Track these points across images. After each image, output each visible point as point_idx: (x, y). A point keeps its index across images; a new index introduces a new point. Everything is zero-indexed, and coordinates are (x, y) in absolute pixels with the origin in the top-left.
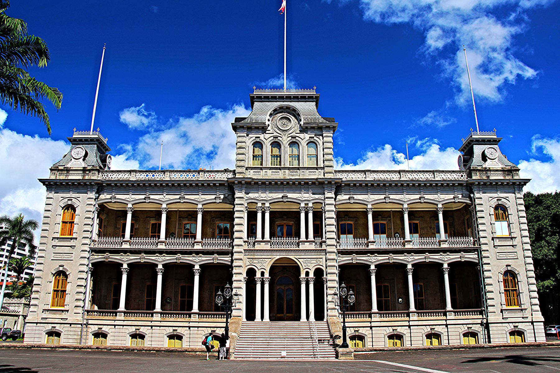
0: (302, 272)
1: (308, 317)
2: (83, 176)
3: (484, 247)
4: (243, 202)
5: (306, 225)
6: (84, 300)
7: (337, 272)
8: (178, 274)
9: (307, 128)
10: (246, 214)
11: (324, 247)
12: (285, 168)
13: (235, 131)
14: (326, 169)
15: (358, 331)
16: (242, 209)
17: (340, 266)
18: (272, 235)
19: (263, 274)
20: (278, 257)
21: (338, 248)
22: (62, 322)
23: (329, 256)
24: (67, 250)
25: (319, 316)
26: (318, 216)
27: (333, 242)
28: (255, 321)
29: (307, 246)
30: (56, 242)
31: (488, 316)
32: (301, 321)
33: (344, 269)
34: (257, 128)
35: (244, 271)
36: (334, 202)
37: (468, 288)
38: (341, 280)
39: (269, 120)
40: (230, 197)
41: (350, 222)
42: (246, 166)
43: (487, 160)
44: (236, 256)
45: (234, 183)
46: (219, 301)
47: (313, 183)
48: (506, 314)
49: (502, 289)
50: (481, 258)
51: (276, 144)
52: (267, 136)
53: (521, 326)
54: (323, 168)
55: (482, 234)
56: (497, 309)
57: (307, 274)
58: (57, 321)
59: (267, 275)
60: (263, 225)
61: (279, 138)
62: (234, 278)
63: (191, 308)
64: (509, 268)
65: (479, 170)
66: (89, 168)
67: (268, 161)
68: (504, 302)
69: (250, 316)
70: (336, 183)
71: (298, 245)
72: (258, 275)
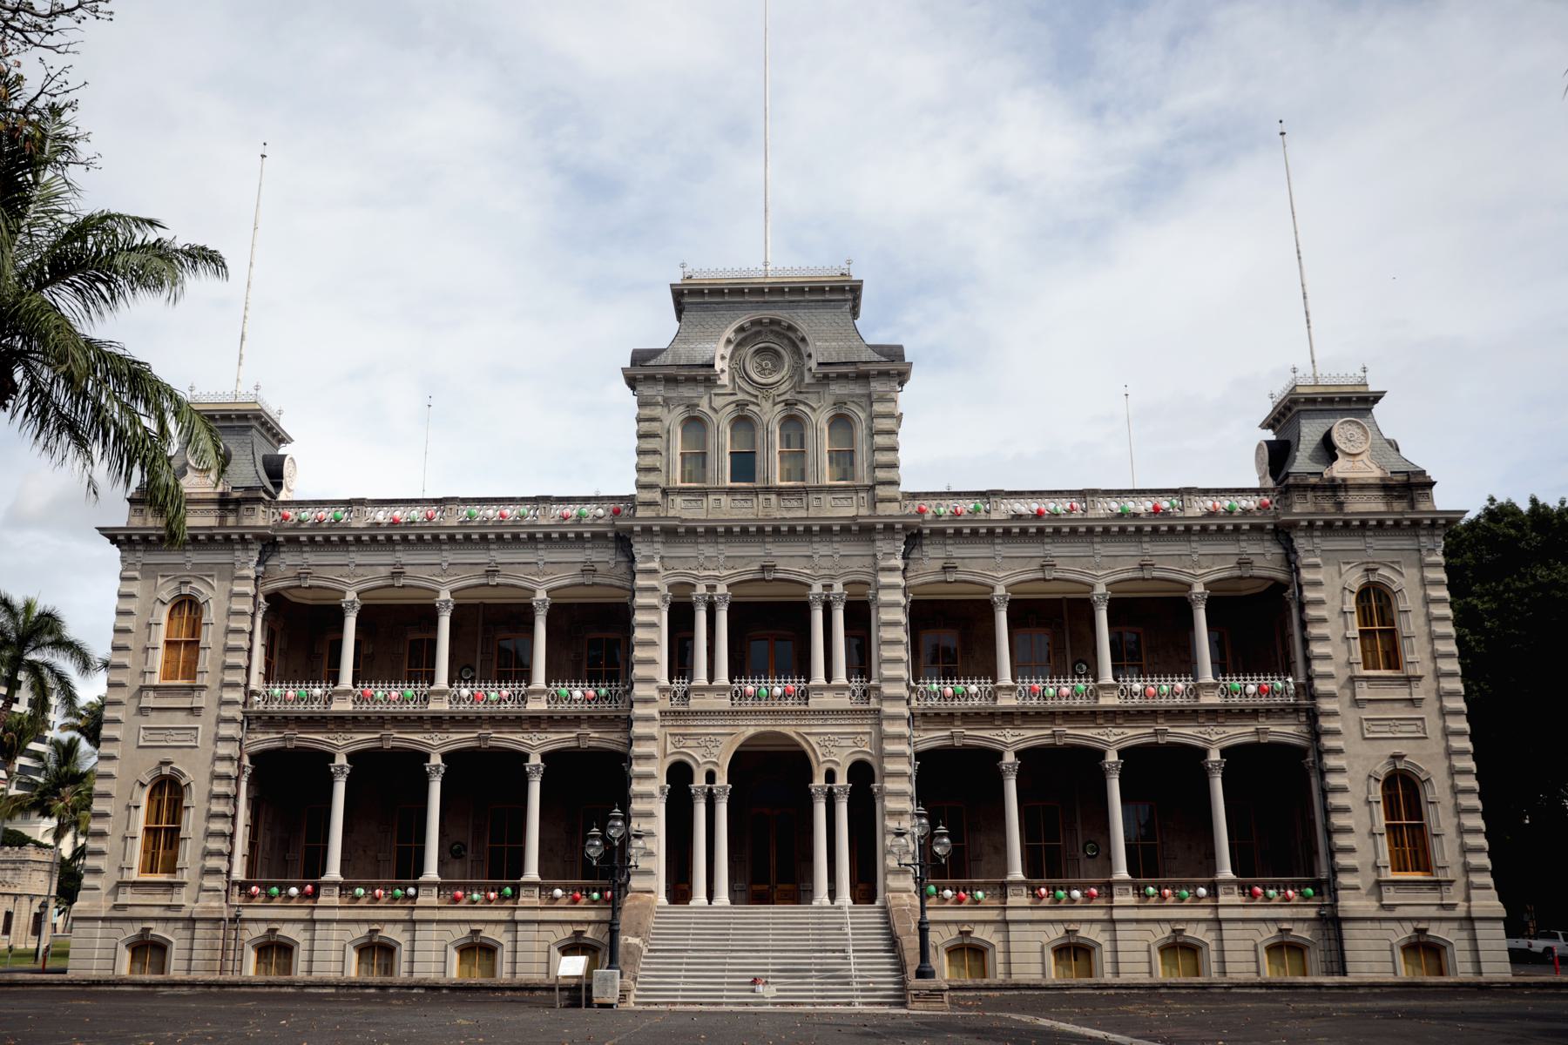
0: (816, 771)
1: (832, 894)
2: (222, 518)
3: (1325, 705)
4: (654, 583)
5: (827, 641)
6: (230, 855)
7: (909, 770)
8: (485, 782)
9: (826, 376)
11: (874, 703)
12: (768, 490)
13: (633, 388)
14: (882, 491)
15: (968, 933)
16: (654, 601)
17: (918, 755)
18: (736, 671)
19: (711, 777)
20: (751, 731)
22: (170, 914)
23: (889, 728)
24: (180, 720)
25: (865, 887)
26: (859, 616)
27: (901, 690)
28: (692, 903)
29: (828, 701)
30: (150, 700)
31: (1336, 900)
32: (815, 903)
33: (928, 761)
34: (692, 380)
35: (659, 769)
36: (902, 582)
37: (1279, 818)
38: (924, 793)
39: (723, 358)
40: (623, 568)
41: (950, 632)
43: (1335, 458)
44: (638, 729)
45: (630, 530)
46: (594, 850)
47: (845, 530)
48: (1391, 896)
49: (1381, 822)
50: (1316, 734)
52: (718, 402)
53: (1435, 931)
54: (872, 488)
55: (1318, 667)
56: (1364, 880)
57: (830, 776)
58: (156, 912)
59: (722, 780)
60: (713, 643)
61: (751, 407)
62: (636, 787)
63: (519, 869)
64: (1401, 765)
65: (1314, 487)
66: (236, 495)
67: (722, 471)
68: (1385, 857)
69: (679, 890)
70: (906, 527)
71: (805, 695)
72: (700, 781)
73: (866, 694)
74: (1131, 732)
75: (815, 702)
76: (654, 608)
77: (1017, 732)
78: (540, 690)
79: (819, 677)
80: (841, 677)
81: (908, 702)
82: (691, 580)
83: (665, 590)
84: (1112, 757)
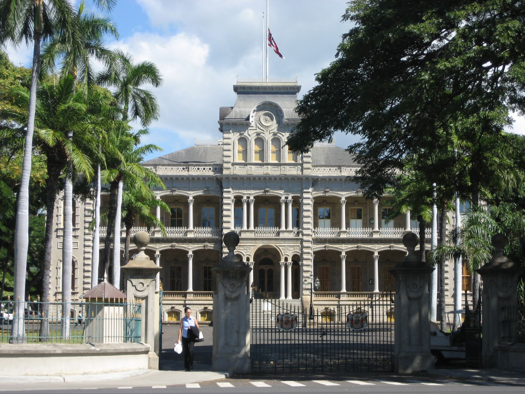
10: (233, 206)
12: (268, 164)
17: (314, 253)
18: (256, 225)
20: (261, 245)
21: (313, 236)
40: (218, 189)
42: (232, 162)
45: (222, 178)
51: (260, 140)
52: (251, 132)
57: (286, 259)
70: (312, 179)
71: (278, 233)
73: (298, 233)
74: (382, 246)
75: (282, 236)
76: (229, 204)
77: (346, 246)
78: (193, 231)
79: (283, 228)
80: (290, 228)
81: (311, 236)
82: (242, 195)
83: (233, 198)
84: (376, 254)
